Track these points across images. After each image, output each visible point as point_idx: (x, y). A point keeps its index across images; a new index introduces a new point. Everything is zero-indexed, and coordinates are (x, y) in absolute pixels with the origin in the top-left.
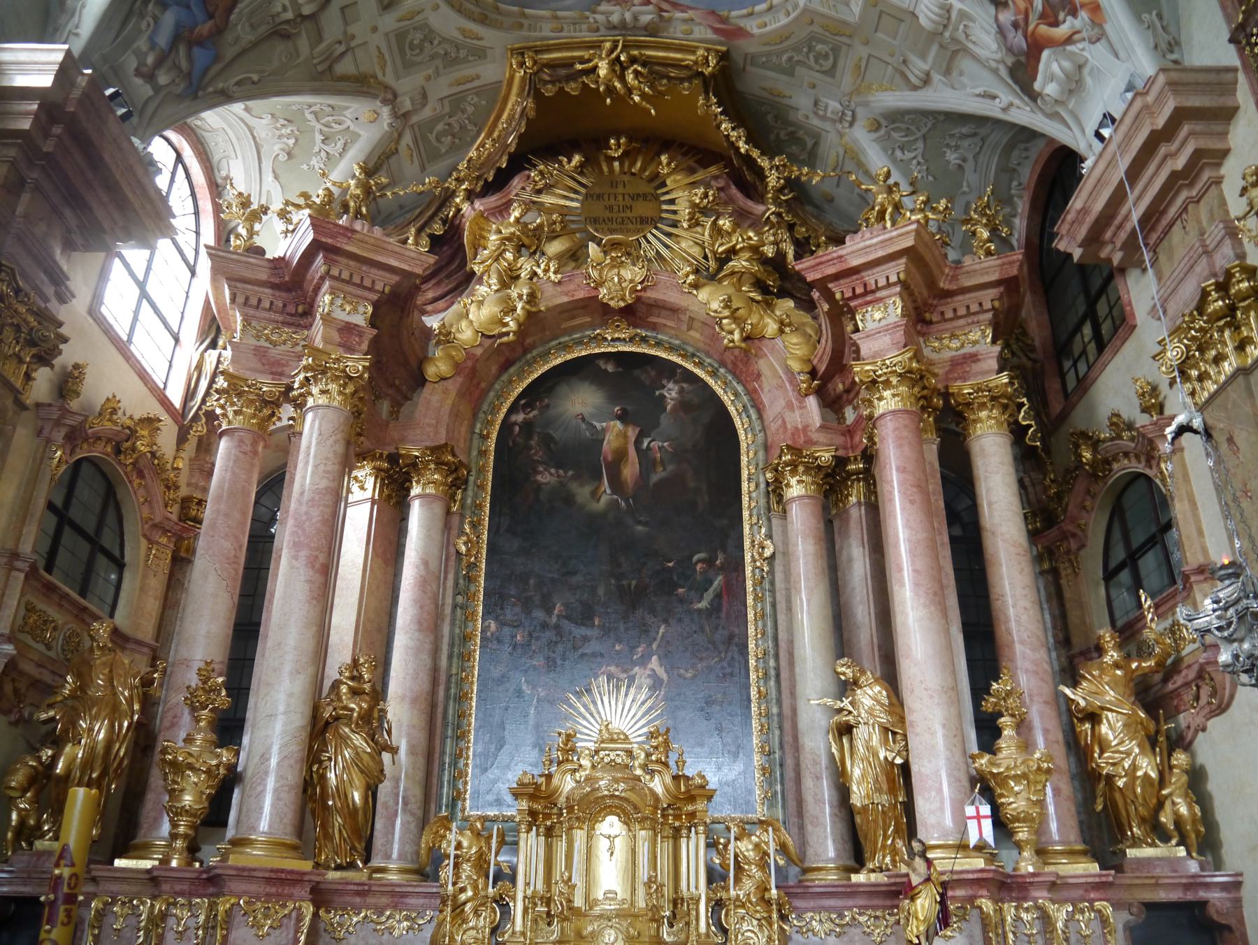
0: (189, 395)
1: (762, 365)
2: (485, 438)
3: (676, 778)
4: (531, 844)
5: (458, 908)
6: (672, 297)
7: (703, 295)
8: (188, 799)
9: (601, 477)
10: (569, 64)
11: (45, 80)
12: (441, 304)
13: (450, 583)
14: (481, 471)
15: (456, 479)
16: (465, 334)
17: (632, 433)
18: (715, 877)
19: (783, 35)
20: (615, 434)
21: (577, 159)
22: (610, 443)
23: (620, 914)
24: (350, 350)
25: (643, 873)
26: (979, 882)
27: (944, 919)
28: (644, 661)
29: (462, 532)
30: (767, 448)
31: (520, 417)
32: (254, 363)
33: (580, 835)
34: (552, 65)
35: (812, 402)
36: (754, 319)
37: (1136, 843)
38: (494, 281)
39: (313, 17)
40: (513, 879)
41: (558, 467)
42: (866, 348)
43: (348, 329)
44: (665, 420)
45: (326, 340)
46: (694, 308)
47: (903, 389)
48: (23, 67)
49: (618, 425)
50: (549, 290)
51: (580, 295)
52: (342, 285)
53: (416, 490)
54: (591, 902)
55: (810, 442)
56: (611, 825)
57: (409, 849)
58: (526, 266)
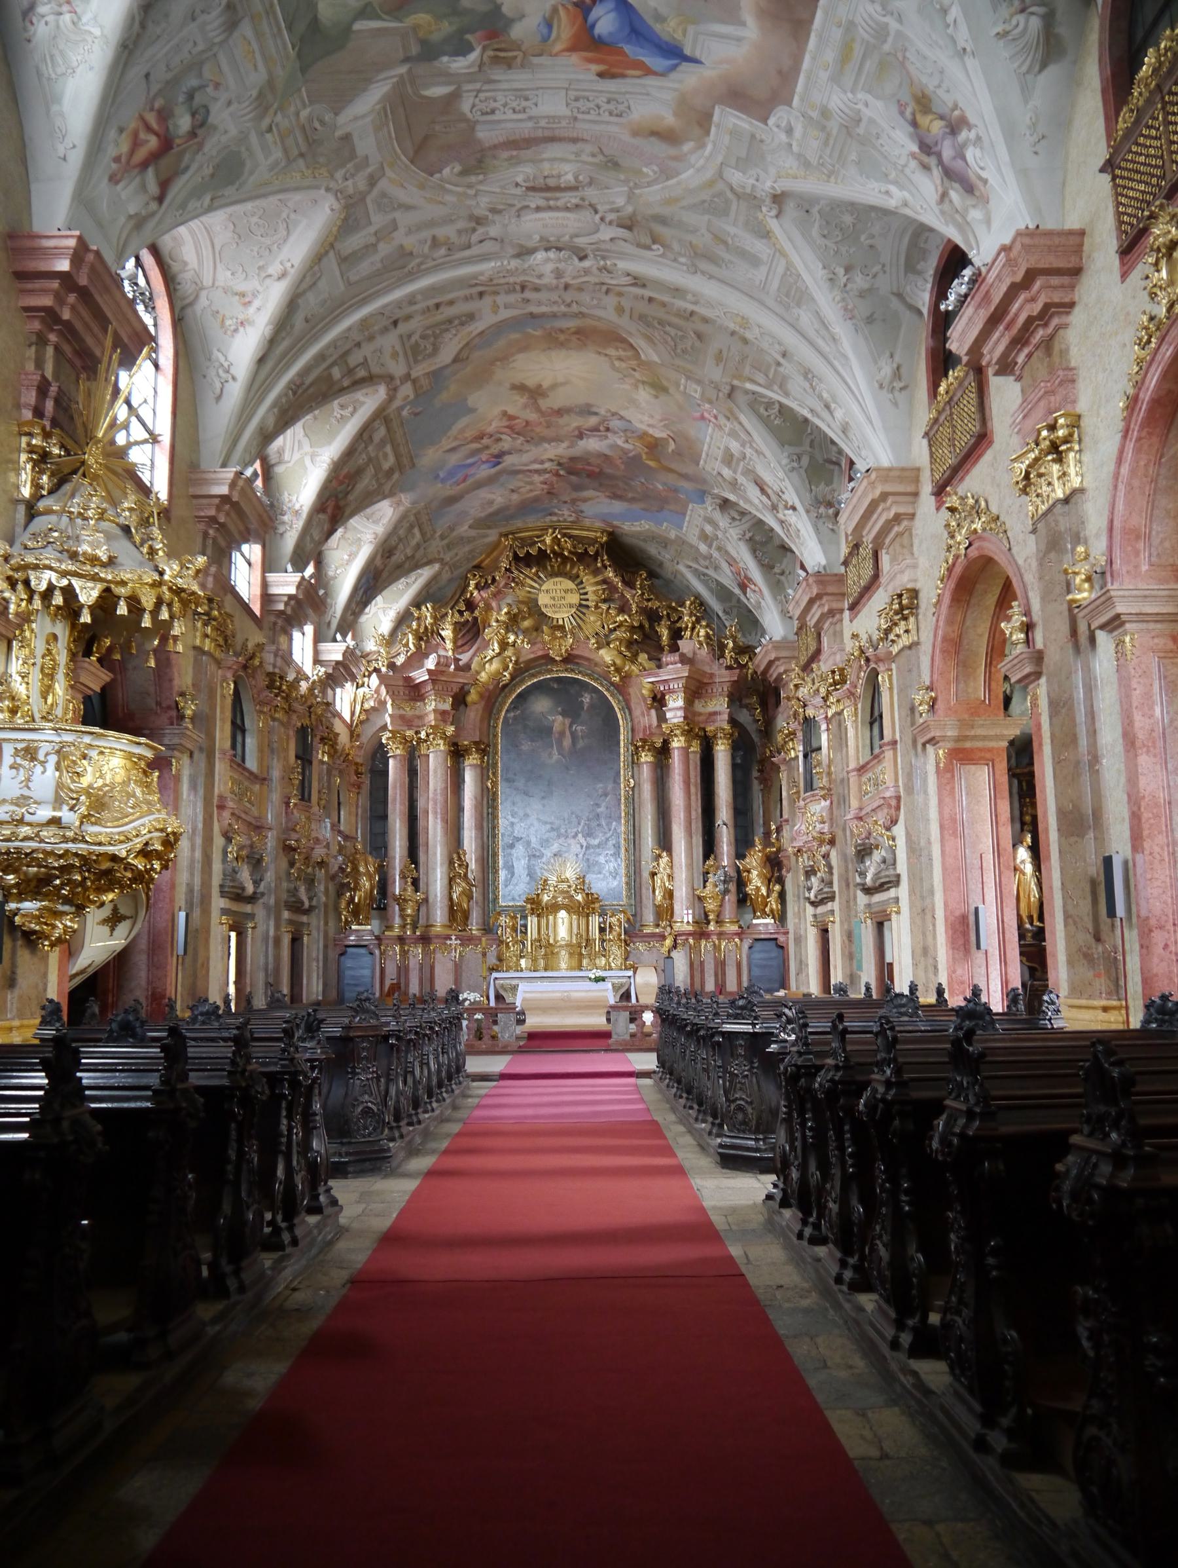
0: (353, 714)
1: (631, 690)
2: (495, 727)
3: (587, 894)
4: (532, 921)
5: (507, 944)
6: (586, 654)
7: (602, 652)
8: (409, 911)
9: (552, 747)
10: (531, 537)
11: (339, 658)
12: (466, 648)
13: (485, 802)
14: (496, 745)
15: (484, 749)
16: (483, 677)
17: (567, 721)
18: (602, 930)
19: (640, 533)
20: (559, 722)
21: (534, 570)
22: (557, 727)
23: (567, 945)
24: (445, 721)
25: (575, 931)
26: (689, 934)
27: (675, 947)
28: (575, 836)
29: (488, 778)
30: (633, 730)
31: (512, 714)
32: (400, 722)
33: (551, 918)
34: (521, 539)
35: (653, 712)
36: (627, 668)
37: (758, 918)
38: (496, 646)
39: (413, 556)
40: (526, 933)
41: (532, 741)
42: (669, 715)
43: (444, 713)
44: (584, 716)
45: (435, 719)
46: (597, 660)
47: (682, 739)
48: (329, 652)
49: (560, 718)
50: (524, 652)
51: (540, 653)
52: (440, 695)
53: (467, 763)
54: (556, 941)
55: (651, 734)
56: (563, 914)
57: (480, 921)
58: (512, 638)
